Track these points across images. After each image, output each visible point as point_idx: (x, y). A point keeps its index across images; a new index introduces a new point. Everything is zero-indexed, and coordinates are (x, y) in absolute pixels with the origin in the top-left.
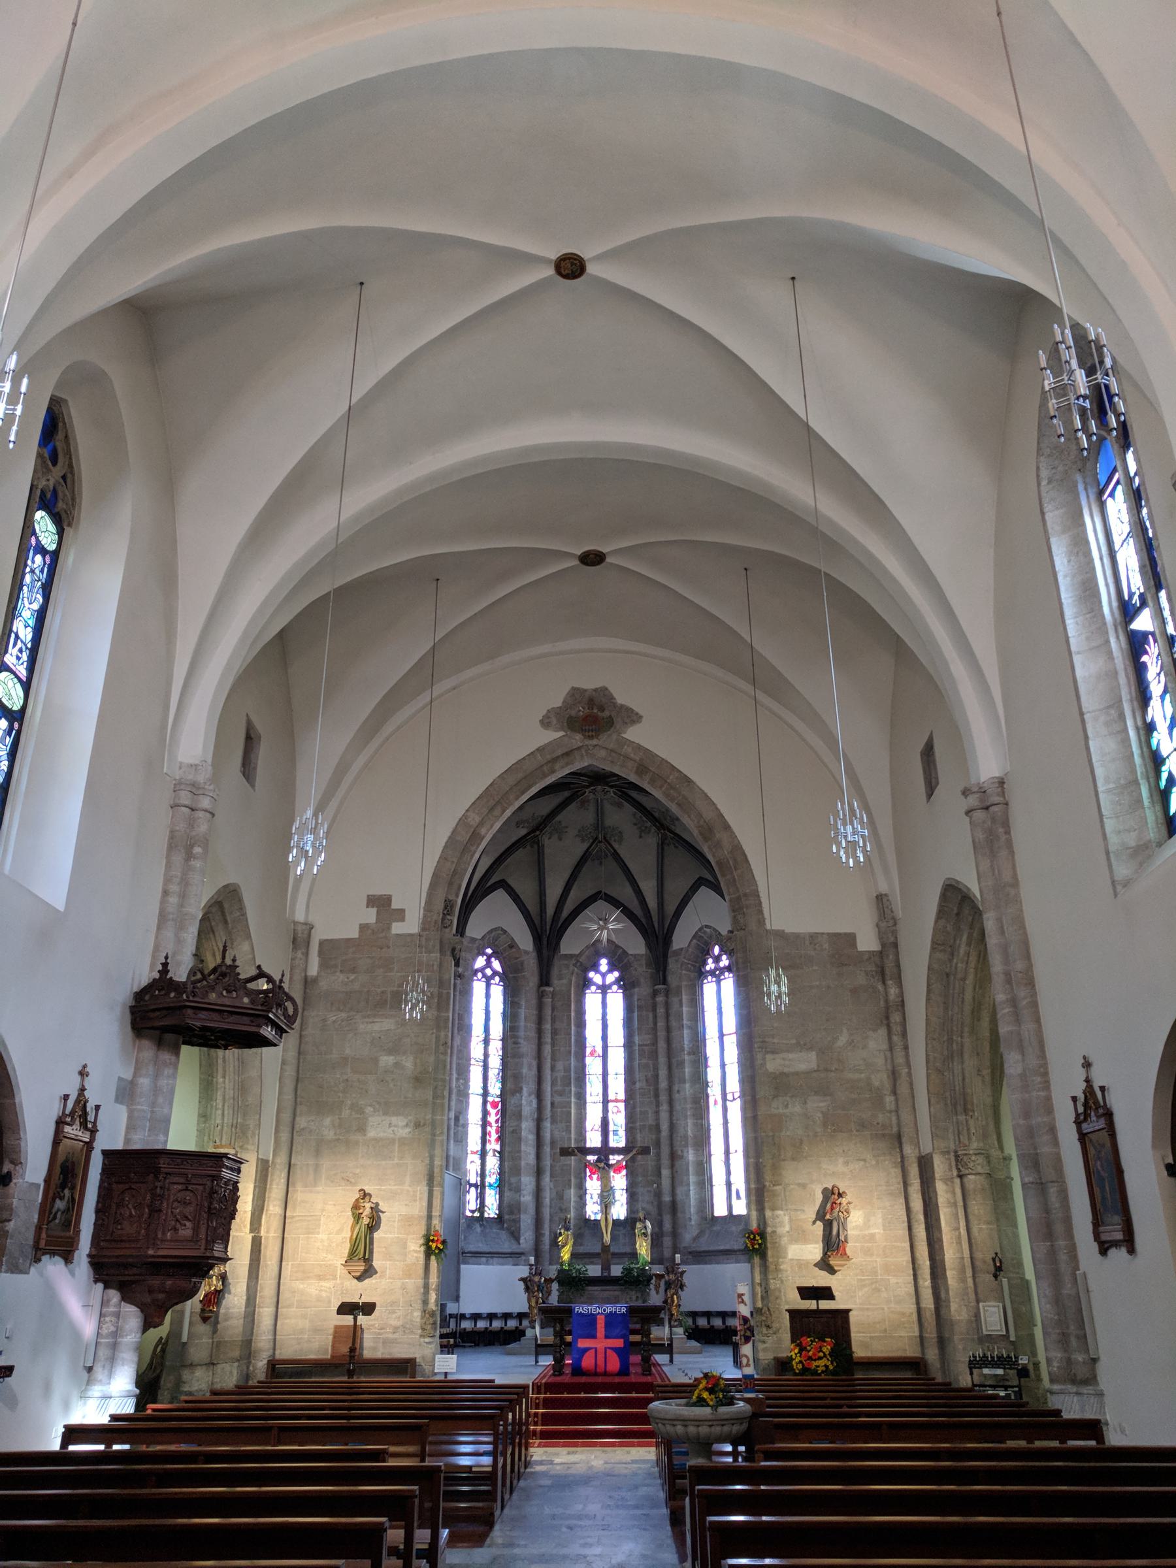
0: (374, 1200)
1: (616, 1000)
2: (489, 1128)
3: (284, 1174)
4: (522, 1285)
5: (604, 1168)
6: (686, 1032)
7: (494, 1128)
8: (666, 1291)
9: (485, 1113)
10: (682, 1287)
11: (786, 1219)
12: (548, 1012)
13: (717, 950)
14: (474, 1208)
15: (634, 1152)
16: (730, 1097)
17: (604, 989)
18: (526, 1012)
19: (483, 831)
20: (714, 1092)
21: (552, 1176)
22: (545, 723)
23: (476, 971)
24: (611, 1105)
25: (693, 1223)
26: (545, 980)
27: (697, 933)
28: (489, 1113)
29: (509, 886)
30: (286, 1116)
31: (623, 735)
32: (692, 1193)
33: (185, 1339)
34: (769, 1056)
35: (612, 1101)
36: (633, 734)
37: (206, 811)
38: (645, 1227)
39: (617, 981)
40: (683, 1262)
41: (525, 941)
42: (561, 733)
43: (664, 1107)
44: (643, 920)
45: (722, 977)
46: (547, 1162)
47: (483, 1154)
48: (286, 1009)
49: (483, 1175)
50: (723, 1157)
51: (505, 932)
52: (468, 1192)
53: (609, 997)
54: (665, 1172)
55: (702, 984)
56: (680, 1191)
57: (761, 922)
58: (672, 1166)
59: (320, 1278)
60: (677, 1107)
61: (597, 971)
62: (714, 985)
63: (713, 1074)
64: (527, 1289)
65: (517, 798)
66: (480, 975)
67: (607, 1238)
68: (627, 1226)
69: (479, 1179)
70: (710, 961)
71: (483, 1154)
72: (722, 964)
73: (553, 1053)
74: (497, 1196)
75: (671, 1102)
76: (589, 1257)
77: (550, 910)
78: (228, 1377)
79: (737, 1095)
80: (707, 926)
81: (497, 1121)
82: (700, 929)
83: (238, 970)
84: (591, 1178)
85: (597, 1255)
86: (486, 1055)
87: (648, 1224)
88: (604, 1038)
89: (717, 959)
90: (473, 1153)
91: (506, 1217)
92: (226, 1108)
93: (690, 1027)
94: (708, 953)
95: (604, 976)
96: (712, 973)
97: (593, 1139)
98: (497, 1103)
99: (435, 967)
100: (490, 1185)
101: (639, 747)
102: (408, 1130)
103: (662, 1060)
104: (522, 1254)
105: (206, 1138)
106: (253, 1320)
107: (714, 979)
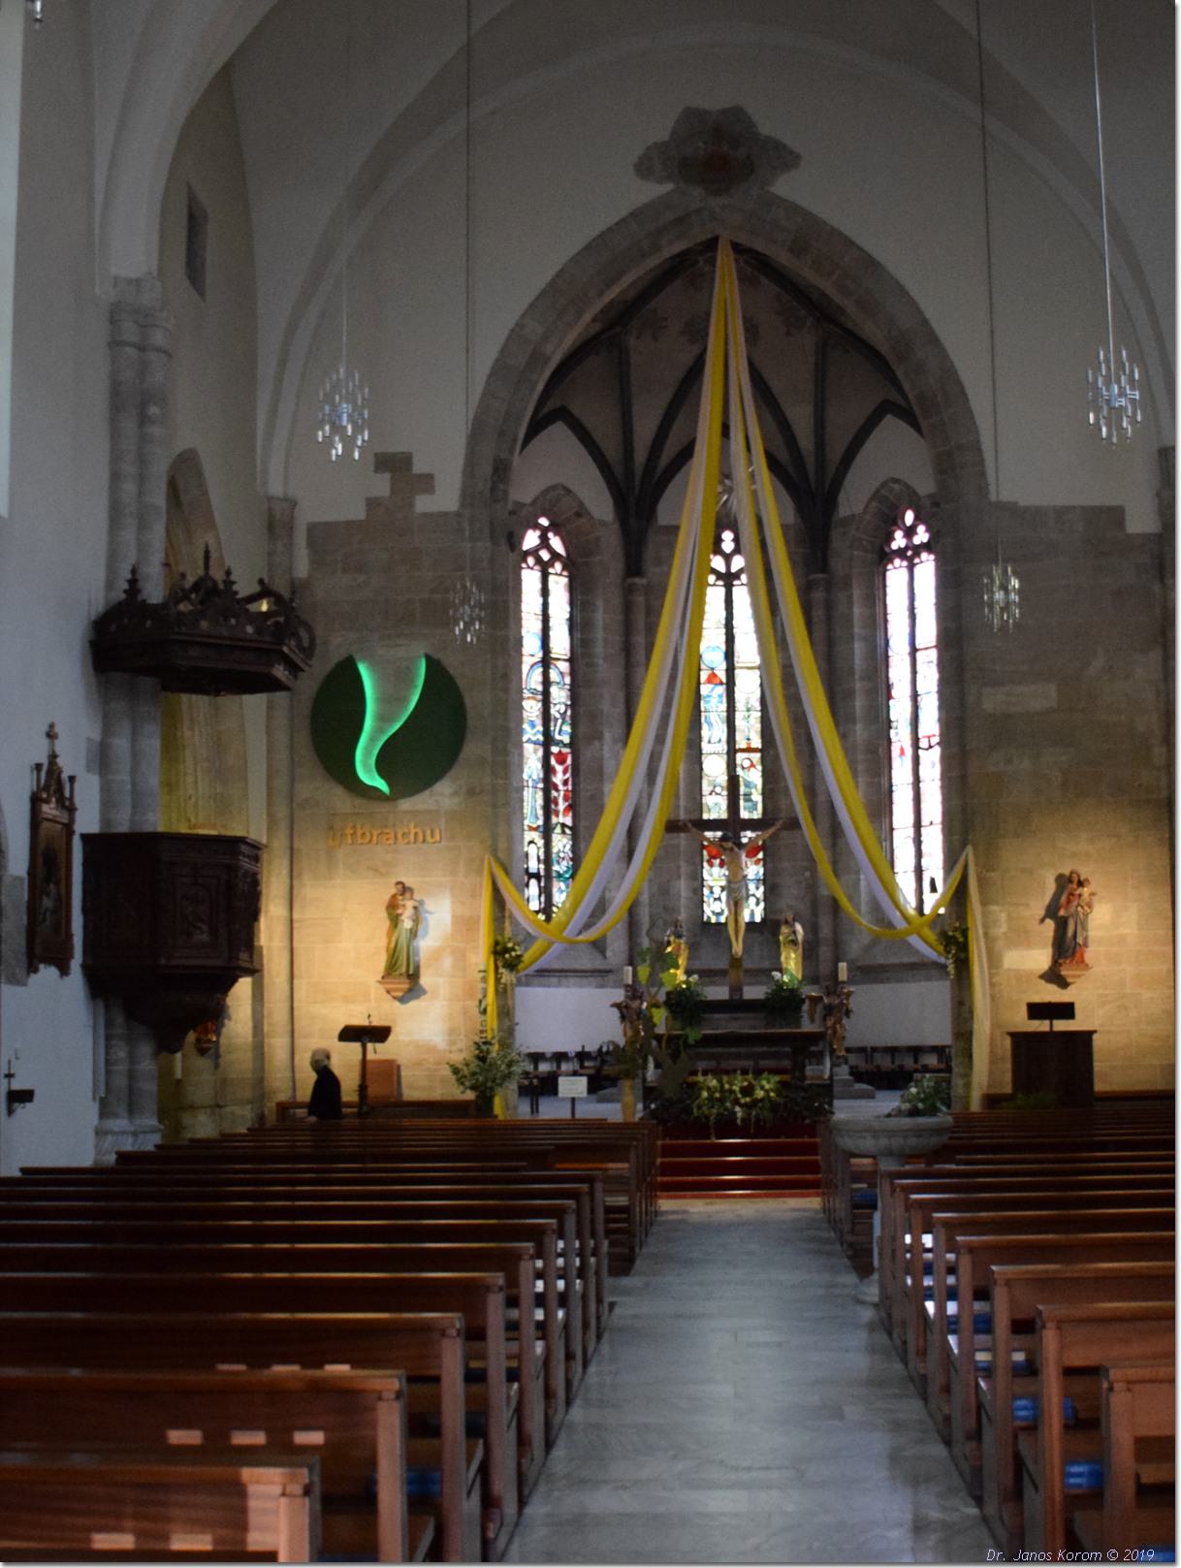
0: (417, 896)
2: (554, 794)
3: (286, 862)
4: (616, 1013)
5: (732, 850)
6: (858, 647)
7: (562, 793)
9: (548, 770)
10: (848, 1013)
11: (1003, 916)
13: (909, 517)
14: (537, 909)
15: (779, 824)
16: (923, 743)
17: (728, 579)
18: (603, 617)
19: (549, 348)
20: (900, 736)
22: (644, 168)
23: (527, 553)
24: (740, 757)
26: (634, 566)
27: (878, 491)
28: (554, 771)
29: (572, 416)
30: (281, 783)
31: (773, 189)
33: (179, 1074)
34: (987, 690)
36: (785, 186)
37: (159, 350)
38: (794, 932)
40: (851, 981)
41: (600, 505)
42: (669, 187)
44: (791, 470)
45: (917, 561)
47: (547, 832)
48: (299, 640)
49: (548, 861)
50: (911, 832)
51: (568, 491)
52: (527, 885)
55: (885, 570)
57: (983, 489)
59: (347, 999)
61: (718, 551)
62: (904, 573)
63: (899, 709)
64: (623, 1018)
65: (601, 293)
66: (531, 561)
67: (738, 948)
68: (767, 931)
69: (542, 866)
70: (899, 535)
71: (547, 832)
72: (917, 540)
76: (708, 975)
77: (640, 456)
78: (241, 1118)
79: (935, 740)
80: (896, 481)
81: (565, 783)
82: (884, 484)
83: (235, 588)
84: (711, 865)
85: (723, 973)
86: (547, 683)
87: (799, 927)
88: (729, 655)
89: (910, 532)
90: (531, 829)
92: (199, 774)
93: (865, 639)
94: (895, 524)
95: (728, 558)
96: (901, 553)
97: (715, 806)
99: (485, 564)
100: (560, 875)
101: (794, 209)
102: (456, 800)
104: (609, 971)
105: (174, 815)
106: (263, 1054)
107: (905, 563)
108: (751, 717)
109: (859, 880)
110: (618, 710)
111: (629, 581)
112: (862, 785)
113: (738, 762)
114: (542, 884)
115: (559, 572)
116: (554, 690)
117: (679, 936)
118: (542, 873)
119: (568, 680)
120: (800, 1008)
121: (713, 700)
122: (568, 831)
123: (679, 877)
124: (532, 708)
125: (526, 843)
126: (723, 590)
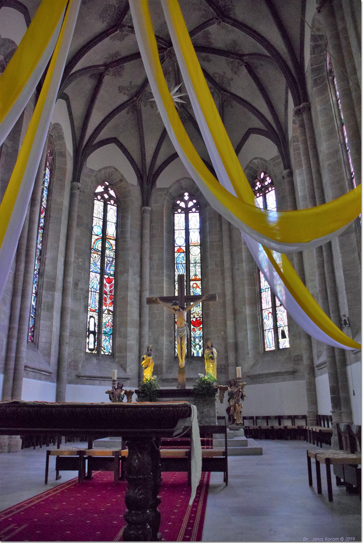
1: (195, 218)
8: (229, 401)
10: (242, 397)
12: (147, 223)
17: (187, 211)
18: (132, 221)
21: (150, 328)
23: (96, 195)
24: (192, 283)
25: (250, 356)
28: (106, 286)
29: (118, 141)
32: (249, 335)
35: (193, 280)
38: (212, 353)
39: (195, 206)
41: (132, 178)
43: (228, 280)
45: (267, 191)
46: (146, 319)
47: (100, 313)
51: (117, 170)
52: (88, 337)
53: (190, 215)
54: (230, 323)
56: (240, 336)
58: (235, 319)
60: (238, 279)
61: (182, 200)
69: (96, 328)
70: (258, 183)
71: (100, 313)
72: (266, 183)
73: (151, 248)
74: (111, 341)
75: (233, 278)
77: (149, 160)
80: (255, 158)
81: (111, 292)
82: (250, 162)
86: (104, 248)
87: (214, 350)
89: (263, 181)
91: (117, 354)
94: (256, 178)
95: (186, 203)
96: (260, 190)
98: (112, 279)
100: (106, 333)
103: (226, 249)
104: (128, 379)
107: (261, 194)
108: (197, 265)
109: (247, 334)
110: (137, 261)
111: (143, 208)
112: (243, 240)
113: (191, 284)
114: (96, 337)
115: (112, 203)
116: (107, 252)
117: (149, 355)
118: (97, 331)
119: (114, 248)
120: (214, 394)
121: (180, 258)
122: (111, 313)
123: (163, 336)
124: (95, 258)
125: (88, 317)
126: (183, 215)
